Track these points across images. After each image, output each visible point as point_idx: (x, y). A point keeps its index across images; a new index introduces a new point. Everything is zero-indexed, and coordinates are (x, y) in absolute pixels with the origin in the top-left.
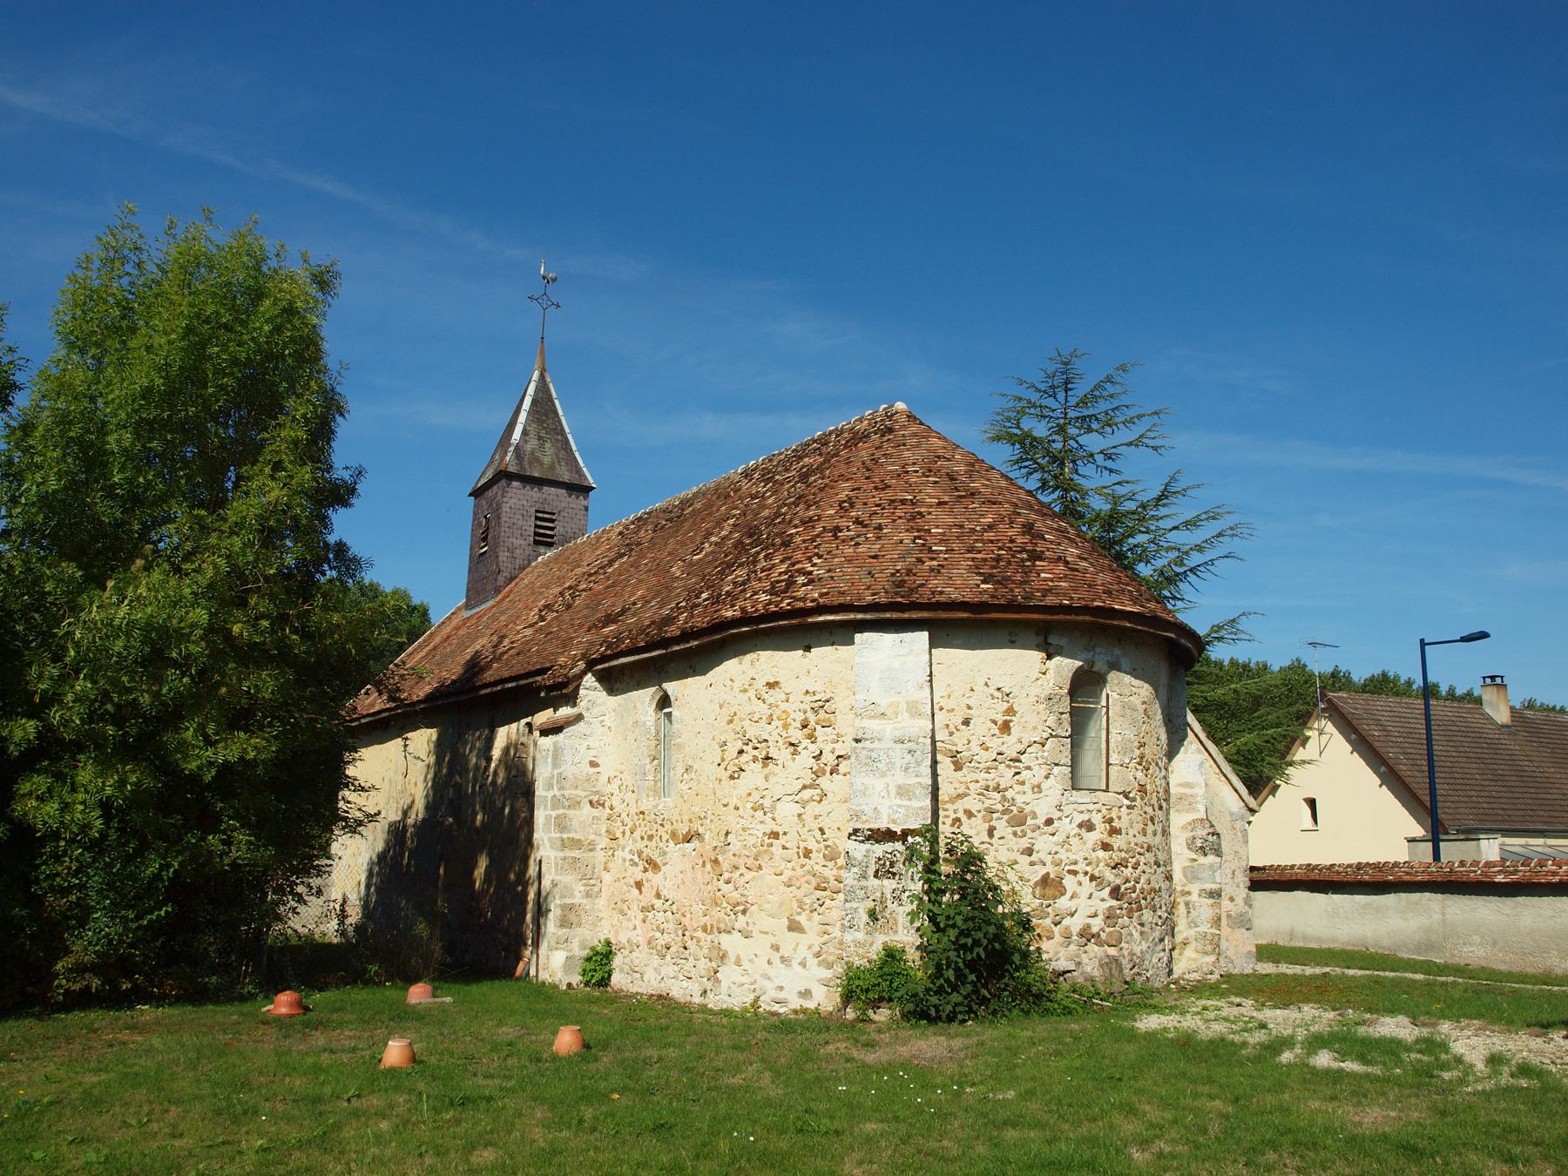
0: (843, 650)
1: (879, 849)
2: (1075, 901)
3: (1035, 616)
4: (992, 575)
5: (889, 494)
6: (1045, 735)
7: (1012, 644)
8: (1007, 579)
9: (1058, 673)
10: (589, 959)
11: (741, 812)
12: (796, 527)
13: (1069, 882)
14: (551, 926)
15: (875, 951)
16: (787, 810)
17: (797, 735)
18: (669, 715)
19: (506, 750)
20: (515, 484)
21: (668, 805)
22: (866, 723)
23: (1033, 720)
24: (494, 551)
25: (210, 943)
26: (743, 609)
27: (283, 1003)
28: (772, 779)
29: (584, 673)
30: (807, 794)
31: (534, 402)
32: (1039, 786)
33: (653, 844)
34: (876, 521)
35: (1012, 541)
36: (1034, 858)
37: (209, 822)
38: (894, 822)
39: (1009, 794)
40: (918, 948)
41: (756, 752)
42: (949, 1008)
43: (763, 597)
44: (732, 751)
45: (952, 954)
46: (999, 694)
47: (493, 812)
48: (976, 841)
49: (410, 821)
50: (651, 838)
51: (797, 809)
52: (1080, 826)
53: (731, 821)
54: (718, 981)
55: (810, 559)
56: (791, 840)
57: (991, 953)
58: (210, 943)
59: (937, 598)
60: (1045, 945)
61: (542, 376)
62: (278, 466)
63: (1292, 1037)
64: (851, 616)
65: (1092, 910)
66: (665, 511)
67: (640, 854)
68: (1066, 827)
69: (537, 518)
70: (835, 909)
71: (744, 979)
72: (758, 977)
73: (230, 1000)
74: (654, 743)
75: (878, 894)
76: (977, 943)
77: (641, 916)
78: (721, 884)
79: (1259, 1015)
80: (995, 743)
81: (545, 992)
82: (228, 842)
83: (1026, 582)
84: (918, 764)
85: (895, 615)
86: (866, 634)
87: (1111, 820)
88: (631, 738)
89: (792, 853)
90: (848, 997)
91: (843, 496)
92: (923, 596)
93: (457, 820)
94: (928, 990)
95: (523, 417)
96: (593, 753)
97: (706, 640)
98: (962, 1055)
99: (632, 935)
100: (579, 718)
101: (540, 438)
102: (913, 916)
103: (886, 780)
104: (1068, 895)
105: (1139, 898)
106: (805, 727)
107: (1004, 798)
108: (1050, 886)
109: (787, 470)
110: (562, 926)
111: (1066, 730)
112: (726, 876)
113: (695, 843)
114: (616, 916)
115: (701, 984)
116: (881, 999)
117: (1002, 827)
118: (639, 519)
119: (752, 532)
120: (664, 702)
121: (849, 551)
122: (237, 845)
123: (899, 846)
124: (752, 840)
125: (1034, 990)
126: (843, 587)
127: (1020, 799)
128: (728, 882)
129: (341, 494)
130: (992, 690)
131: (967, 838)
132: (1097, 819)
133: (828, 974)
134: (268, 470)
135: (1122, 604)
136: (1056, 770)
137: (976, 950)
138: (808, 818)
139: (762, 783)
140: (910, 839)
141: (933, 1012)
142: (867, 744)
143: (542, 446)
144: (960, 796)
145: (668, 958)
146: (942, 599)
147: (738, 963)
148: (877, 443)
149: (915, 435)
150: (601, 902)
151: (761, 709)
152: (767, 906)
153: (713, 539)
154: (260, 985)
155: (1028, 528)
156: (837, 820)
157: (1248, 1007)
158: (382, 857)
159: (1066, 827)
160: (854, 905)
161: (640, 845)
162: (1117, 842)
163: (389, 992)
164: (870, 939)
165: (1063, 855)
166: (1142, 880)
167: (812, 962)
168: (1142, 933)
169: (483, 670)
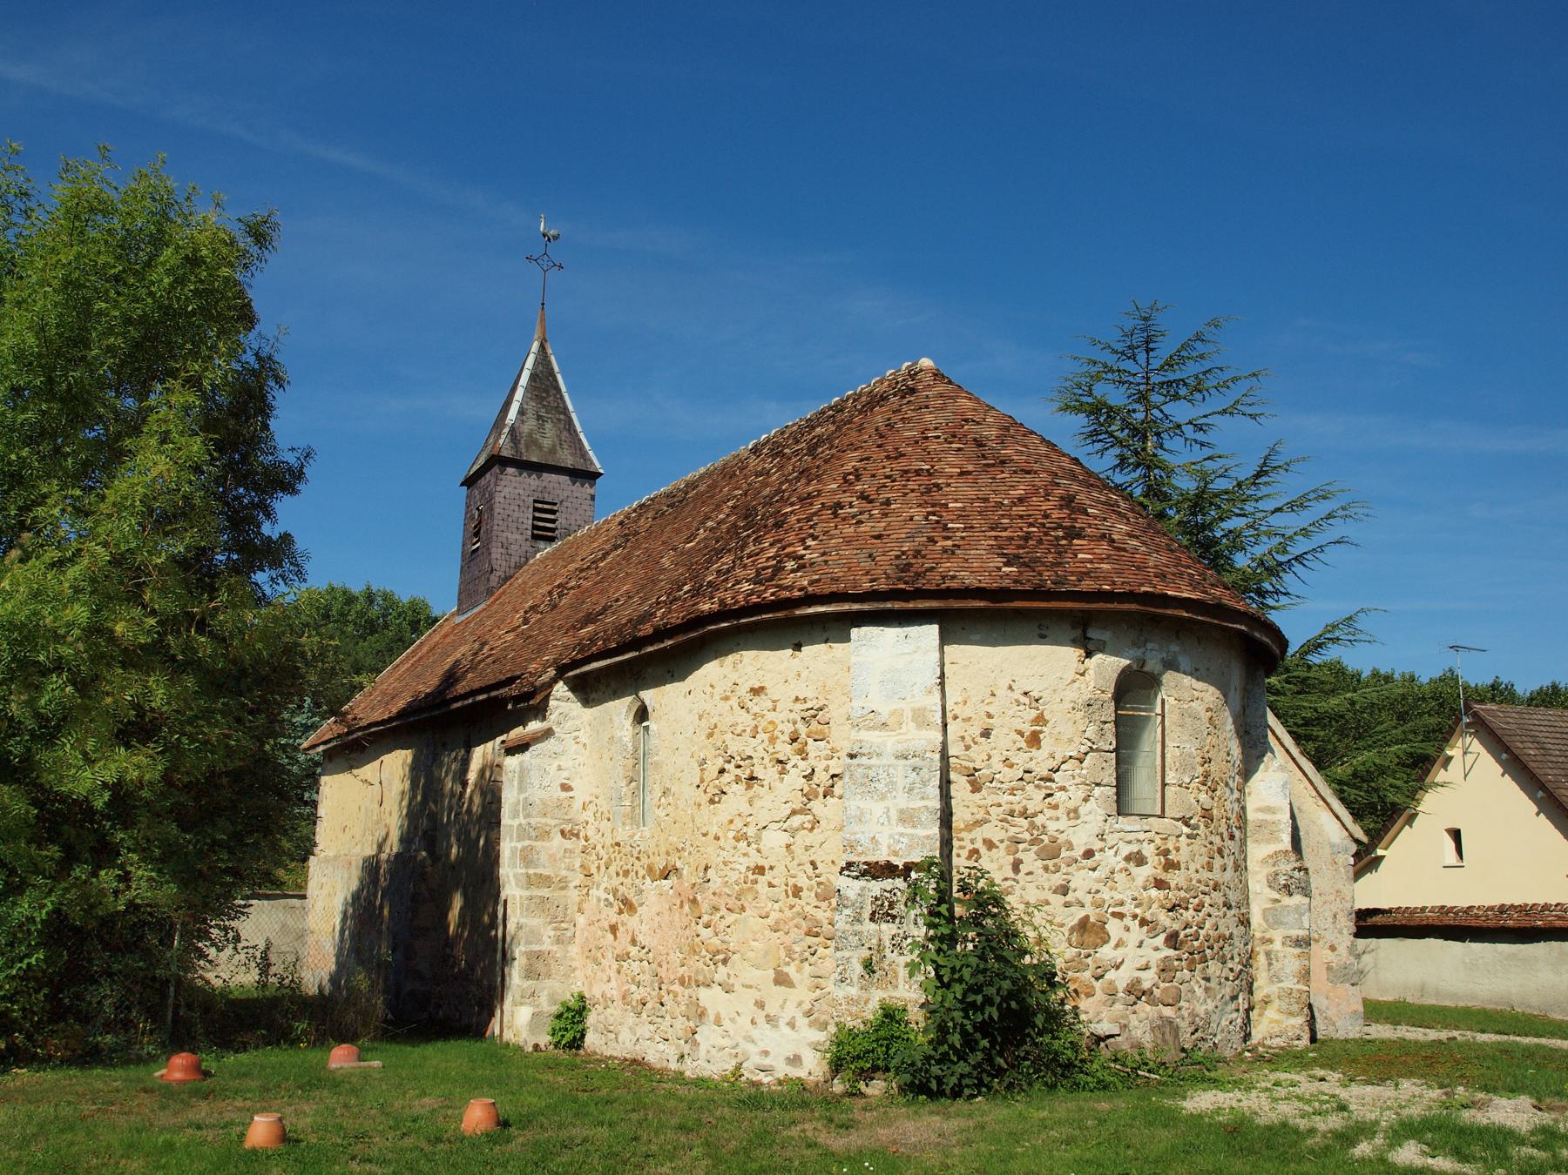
0: (838, 648)
1: (876, 887)
2: (1121, 950)
3: (1069, 605)
4: (1017, 557)
5: (902, 464)
6: (1084, 749)
7: (1042, 638)
8: (1037, 560)
9: (1099, 673)
10: (559, 1017)
11: (722, 842)
12: (792, 504)
13: (1113, 927)
14: (516, 977)
15: (871, 1011)
16: (774, 840)
17: (785, 750)
18: (646, 728)
19: (482, 772)
20: (510, 470)
21: (645, 836)
22: (864, 735)
23: (1068, 730)
24: (487, 547)
25: (105, 997)
26: (722, 601)
27: (176, 1068)
28: (757, 803)
29: (554, 681)
30: (797, 820)
31: (533, 377)
32: (1076, 811)
33: (628, 881)
34: (884, 496)
35: (1046, 516)
36: (1070, 897)
37: (105, 853)
38: (895, 854)
39: (1039, 820)
40: (922, 1006)
41: (738, 771)
42: (954, 1080)
43: (746, 587)
44: (712, 771)
45: (958, 1015)
46: (1026, 700)
47: (468, 844)
48: (997, 877)
49: (384, 856)
50: (626, 873)
51: (785, 838)
52: (1128, 859)
53: (712, 854)
54: (696, 1044)
55: (803, 541)
56: (777, 877)
57: (1005, 1013)
58: (105, 997)
59: (948, 584)
60: (1083, 1004)
61: (542, 347)
62: (165, 438)
63: (1377, 1122)
64: (846, 607)
65: (1143, 962)
66: (668, 495)
67: (615, 892)
68: (1111, 860)
69: (536, 509)
70: (828, 960)
71: (724, 1042)
72: (741, 1040)
73: (126, 1062)
74: (631, 762)
75: (875, 941)
76: (988, 1001)
77: (615, 966)
78: (700, 929)
79: (1343, 1094)
80: (1020, 759)
81: (507, 1054)
82: (125, 878)
83: (1059, 564)
84: (924, 783)
85: (897, 605)
86: (864, 629)
87: (1166, 853)
88: (606, 756)
89: (779, 891)
90: (837, 1066)
91: (848, 468)
92: (931, 582)
93: (431, 853)
94: (928, 1058)
95: (519, 394)
96: (565, 774)
97: (681, 638)
98: (954, 1140)
99: (606, 987)
100: (548, 733)
101: (539, 418)
102: (913, 968)
103: (887, 803)
104: (1113, 942)
105: (1206, 942)
106: (794, 740)
107: (1033, 826)
108: (1089, 932)
109: (797, 442)
110: (527, 977)
111: (1109, 741)
112: (705, 918)
113: (673, 880)
114: (591, 966)
115: (678, 1046)
116: (875, 1069)
117: (1030, 860)
118: (641, 506)
119: (748, 514)
120: (642, 714)
121: (849, 530)
122: (138, 883)
123: (899, 883)
124: (733, 876)
125: (1062, 1059)
126: (838, 572)
127: (1052, 827)
128: (707, 926)
129: (286, 480)
130: (1017, 695)
131: (984, 873)
132: (1148, 851)
133: (821, 1036)
134: (153, 442)
135: (1179, 589)
136: (1097, 791)
137: (988, 1010)
138: (798, 849)
139: (745, 808)
140: (914, 875)
141: (934, 1085)
142: (864, 760)
143: (542, 427)
144: (979, 823)
145: (644, 1015)
146: (954, 584)
147: (718, 1022)
148: (895, 407)
149: (941, 395)
150: (574, 950)
151: (745, 720)
152: (751, 955)
153: (710, 524)
154: (163, 1045)
155: (1068, 501)
156: (831, 853)
157: (1333, 1083)
158: (356, 897)
159: (1111, 860)
160: (846, 954)
161: (616, 882)
162: (1174, 878)
163: (306, 1056)
164: (864, 995)
165: (1106, 895)
166: (1207, 925)
167: (802, 1022)
168: (1207, 990)
169: (457, 681)
